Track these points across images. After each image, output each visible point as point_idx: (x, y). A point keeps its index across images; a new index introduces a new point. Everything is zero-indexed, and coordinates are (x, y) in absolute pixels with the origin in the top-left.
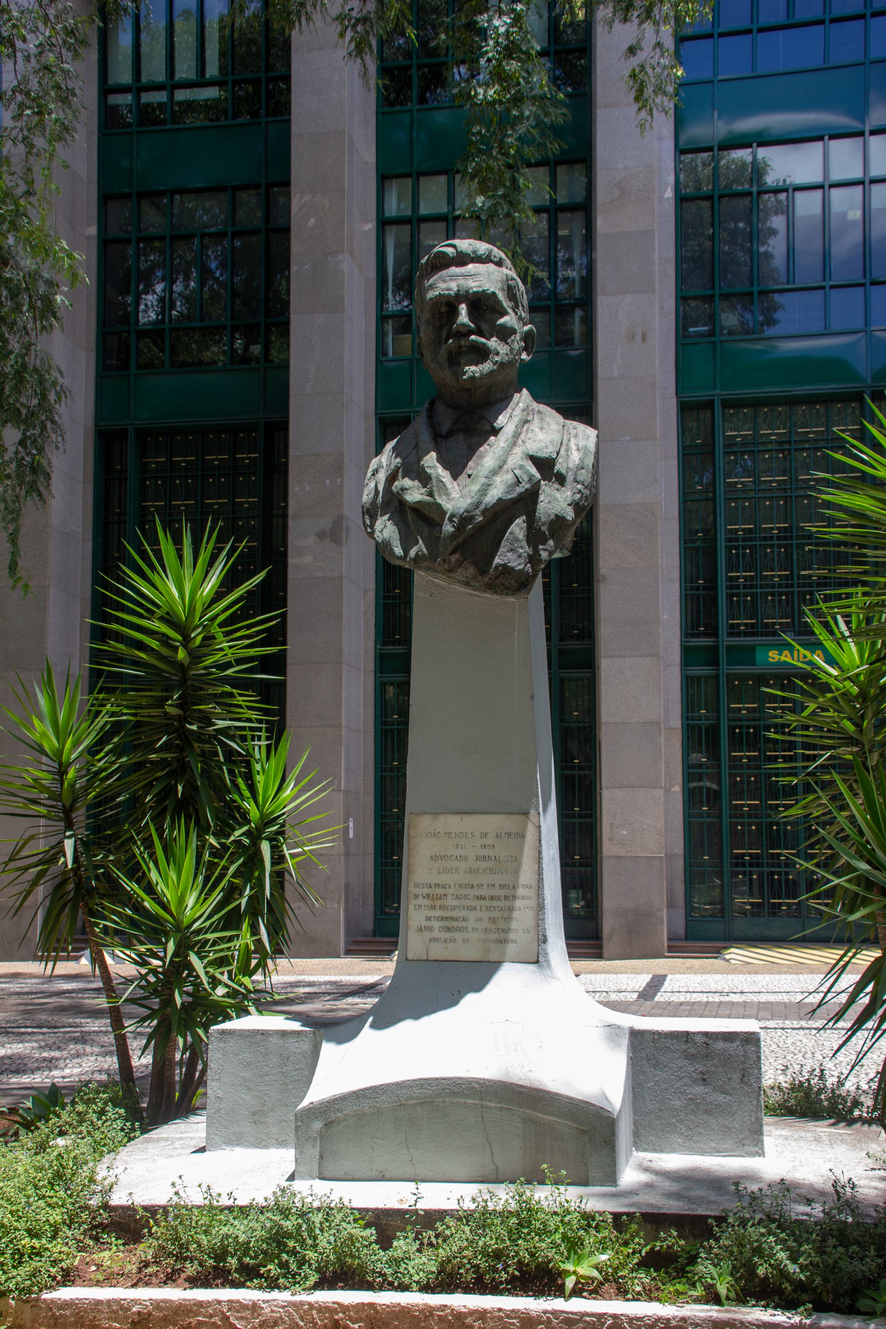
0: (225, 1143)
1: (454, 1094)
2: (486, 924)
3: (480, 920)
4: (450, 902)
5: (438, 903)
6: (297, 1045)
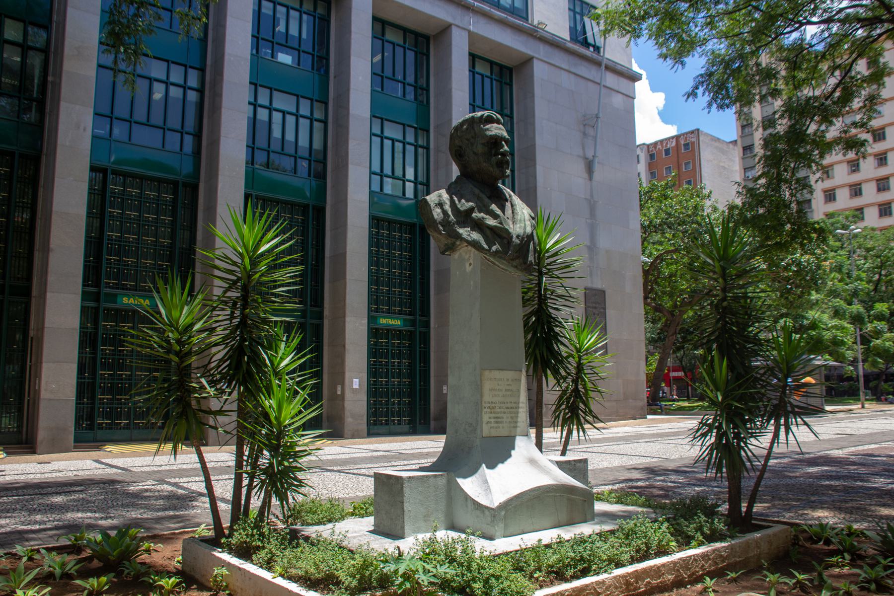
1: (548, 492)
2: (510, 420)
4: (497, 410)
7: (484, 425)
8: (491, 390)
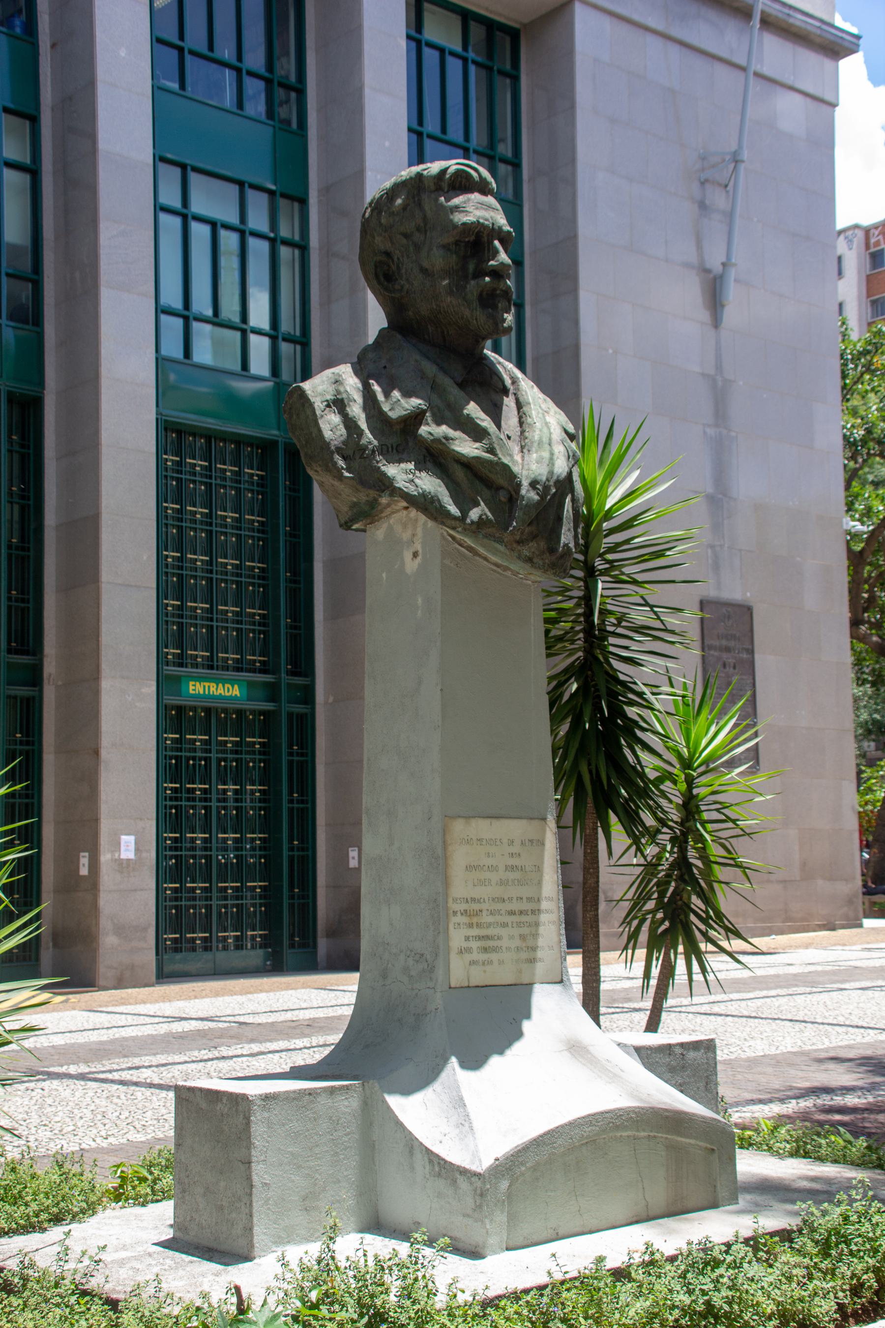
0: (275, 1243)
1: (617, 1128)
2: (517, 942)
3: (511, 937)
4: (486, 918)
5: (475, 920)
6: (346, 1103)
8: (469, 868)
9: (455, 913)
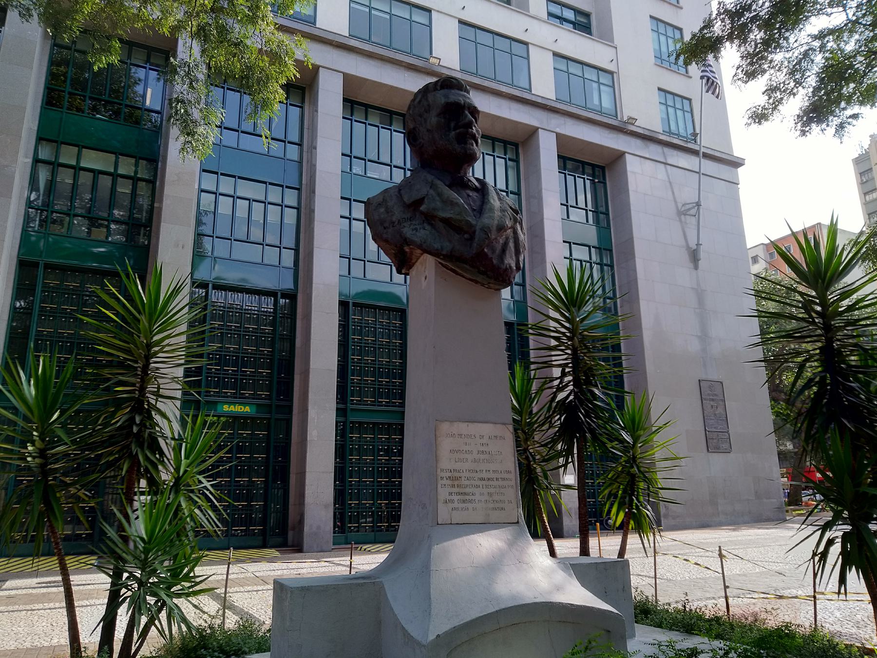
2: (487, 497)
3: (482, 494)
5: (456, 483)
7: (441, 505)
9: (442, 478)
